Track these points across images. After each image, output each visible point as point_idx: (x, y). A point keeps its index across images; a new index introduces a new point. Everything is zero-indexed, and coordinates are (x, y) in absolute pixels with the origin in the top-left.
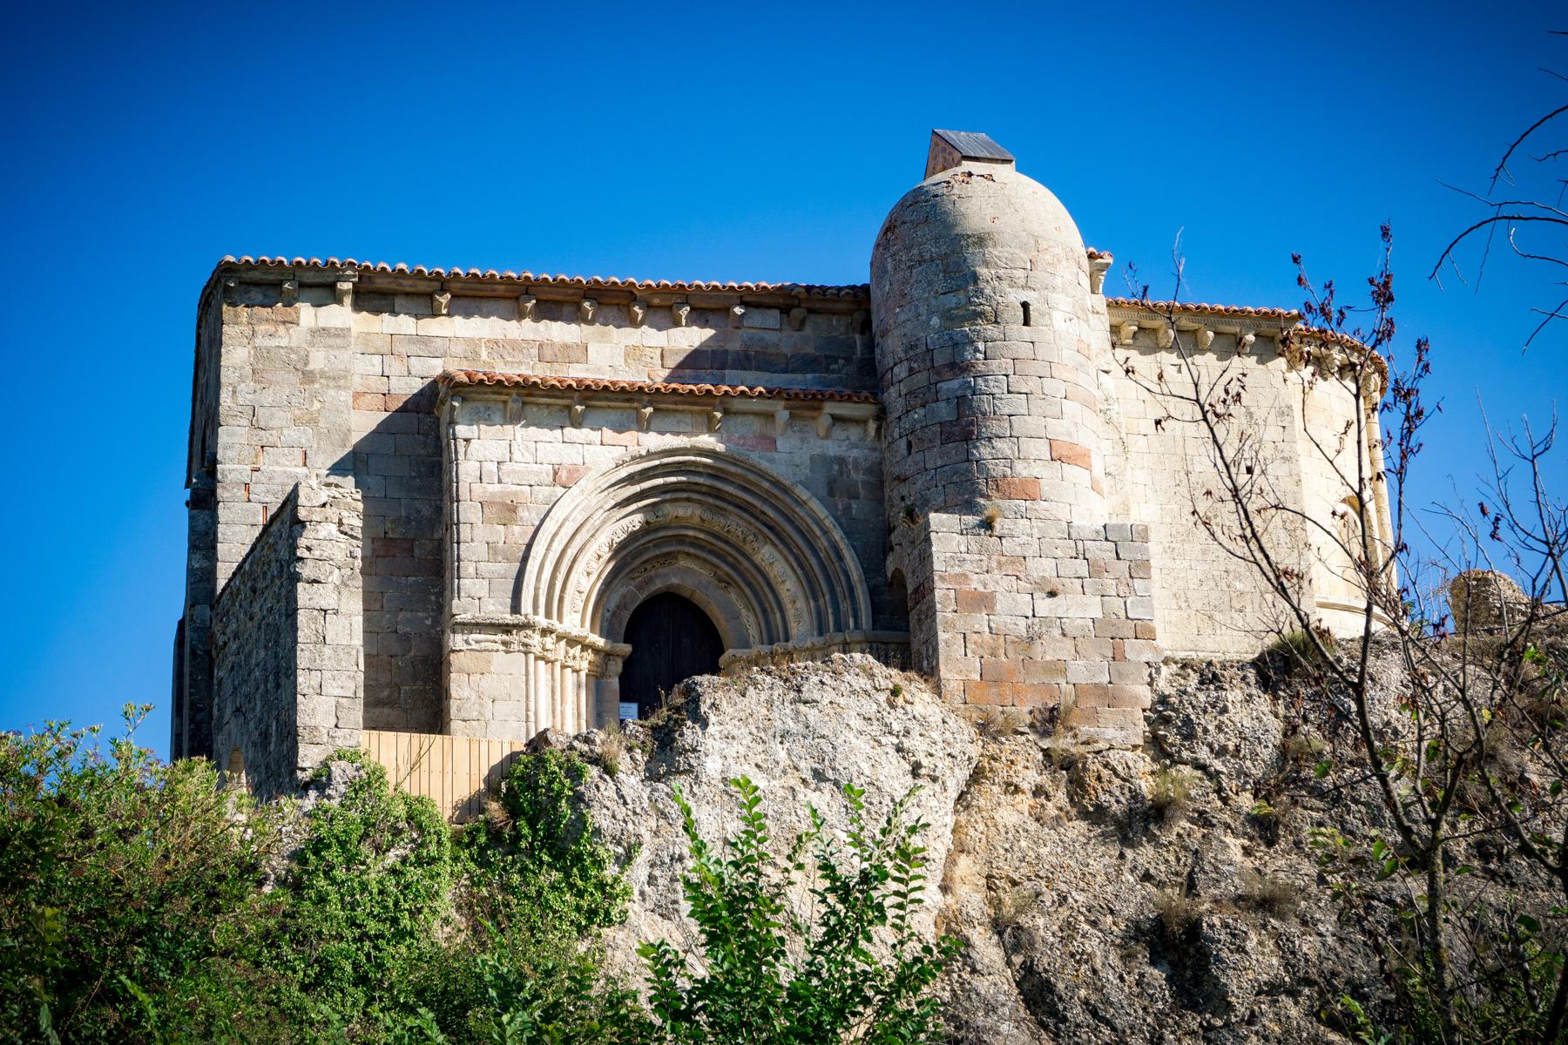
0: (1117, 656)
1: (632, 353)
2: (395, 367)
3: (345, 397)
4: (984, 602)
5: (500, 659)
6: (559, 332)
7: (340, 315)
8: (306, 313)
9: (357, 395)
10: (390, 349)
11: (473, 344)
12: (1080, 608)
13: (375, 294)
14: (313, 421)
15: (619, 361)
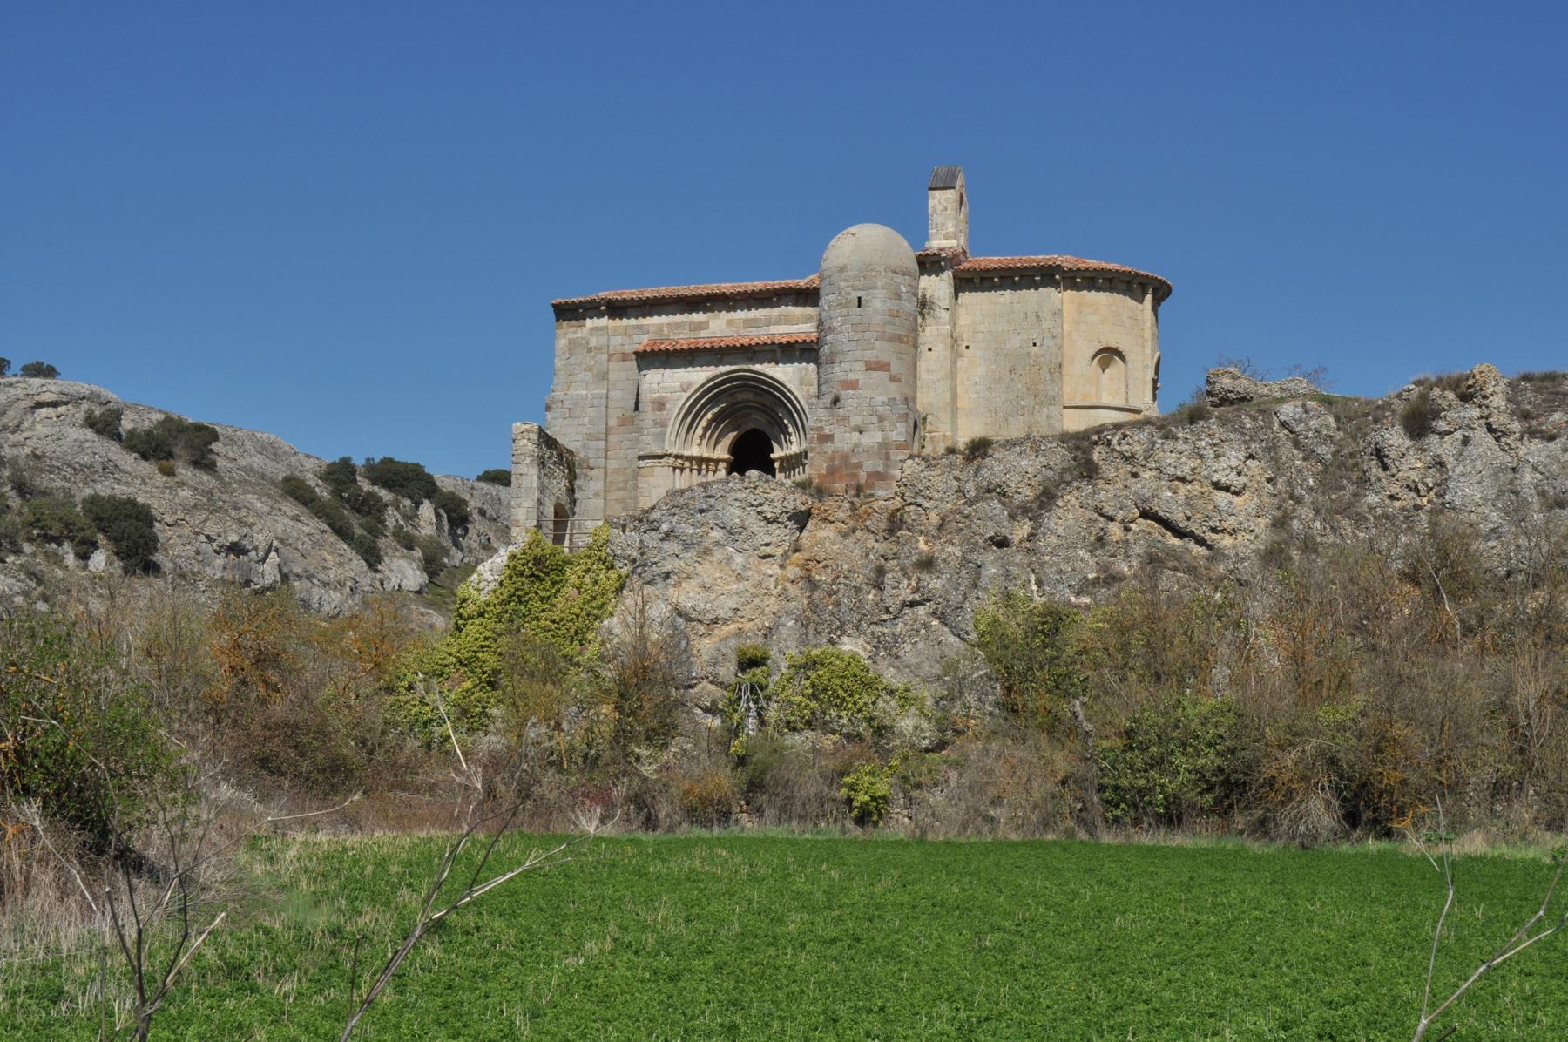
0: (888, 458)
1: (730, 323)
2: (627, 340)
3: (605, 357)
4: (828, 438)
5: (658, 470)
6: (698, 317)
7: (604, 321)
8: (589, 323)
9: (610, 356)
10: (625, 333)
11: (661, 326)
12: (873, 438)
13: (617, 309)
14: (591, 369)
15: (724, 326)
